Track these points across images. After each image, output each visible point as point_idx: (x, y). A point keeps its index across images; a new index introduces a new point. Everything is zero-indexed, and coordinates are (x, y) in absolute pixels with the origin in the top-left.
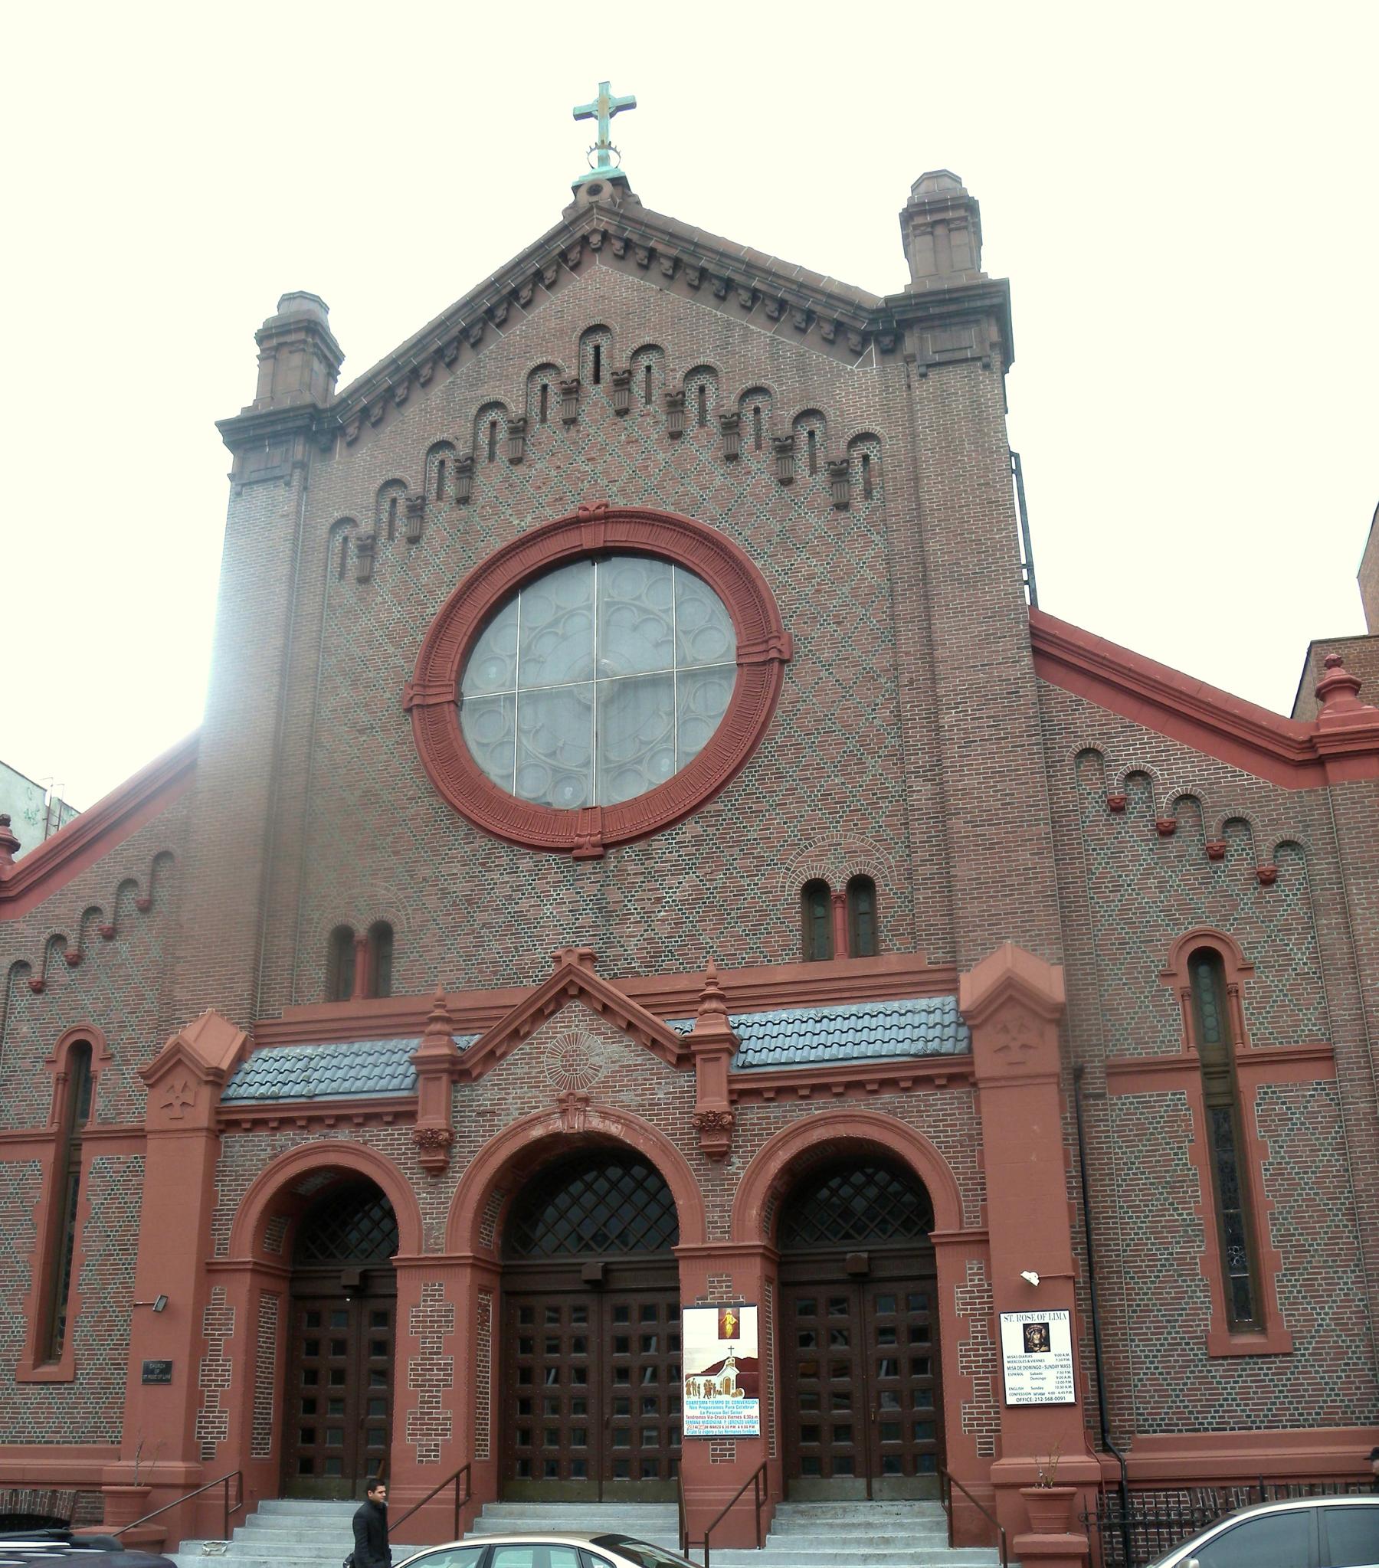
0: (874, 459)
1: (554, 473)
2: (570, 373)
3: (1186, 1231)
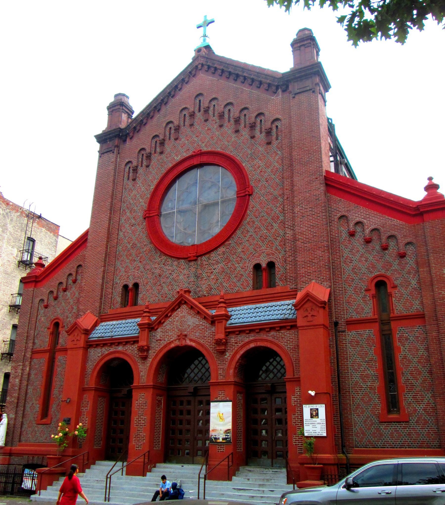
0: (279, 127)
1: (187, 142)
2: (192, 109)
3: (372, 378)
